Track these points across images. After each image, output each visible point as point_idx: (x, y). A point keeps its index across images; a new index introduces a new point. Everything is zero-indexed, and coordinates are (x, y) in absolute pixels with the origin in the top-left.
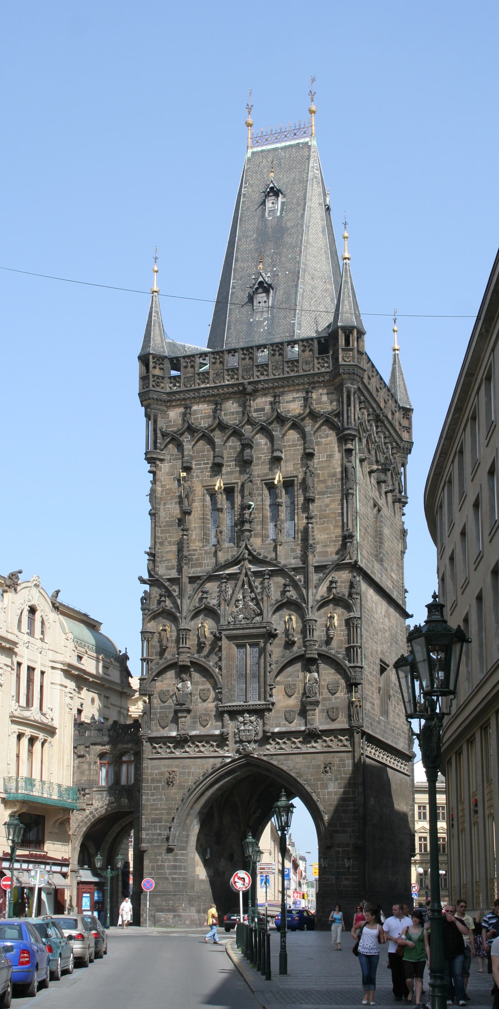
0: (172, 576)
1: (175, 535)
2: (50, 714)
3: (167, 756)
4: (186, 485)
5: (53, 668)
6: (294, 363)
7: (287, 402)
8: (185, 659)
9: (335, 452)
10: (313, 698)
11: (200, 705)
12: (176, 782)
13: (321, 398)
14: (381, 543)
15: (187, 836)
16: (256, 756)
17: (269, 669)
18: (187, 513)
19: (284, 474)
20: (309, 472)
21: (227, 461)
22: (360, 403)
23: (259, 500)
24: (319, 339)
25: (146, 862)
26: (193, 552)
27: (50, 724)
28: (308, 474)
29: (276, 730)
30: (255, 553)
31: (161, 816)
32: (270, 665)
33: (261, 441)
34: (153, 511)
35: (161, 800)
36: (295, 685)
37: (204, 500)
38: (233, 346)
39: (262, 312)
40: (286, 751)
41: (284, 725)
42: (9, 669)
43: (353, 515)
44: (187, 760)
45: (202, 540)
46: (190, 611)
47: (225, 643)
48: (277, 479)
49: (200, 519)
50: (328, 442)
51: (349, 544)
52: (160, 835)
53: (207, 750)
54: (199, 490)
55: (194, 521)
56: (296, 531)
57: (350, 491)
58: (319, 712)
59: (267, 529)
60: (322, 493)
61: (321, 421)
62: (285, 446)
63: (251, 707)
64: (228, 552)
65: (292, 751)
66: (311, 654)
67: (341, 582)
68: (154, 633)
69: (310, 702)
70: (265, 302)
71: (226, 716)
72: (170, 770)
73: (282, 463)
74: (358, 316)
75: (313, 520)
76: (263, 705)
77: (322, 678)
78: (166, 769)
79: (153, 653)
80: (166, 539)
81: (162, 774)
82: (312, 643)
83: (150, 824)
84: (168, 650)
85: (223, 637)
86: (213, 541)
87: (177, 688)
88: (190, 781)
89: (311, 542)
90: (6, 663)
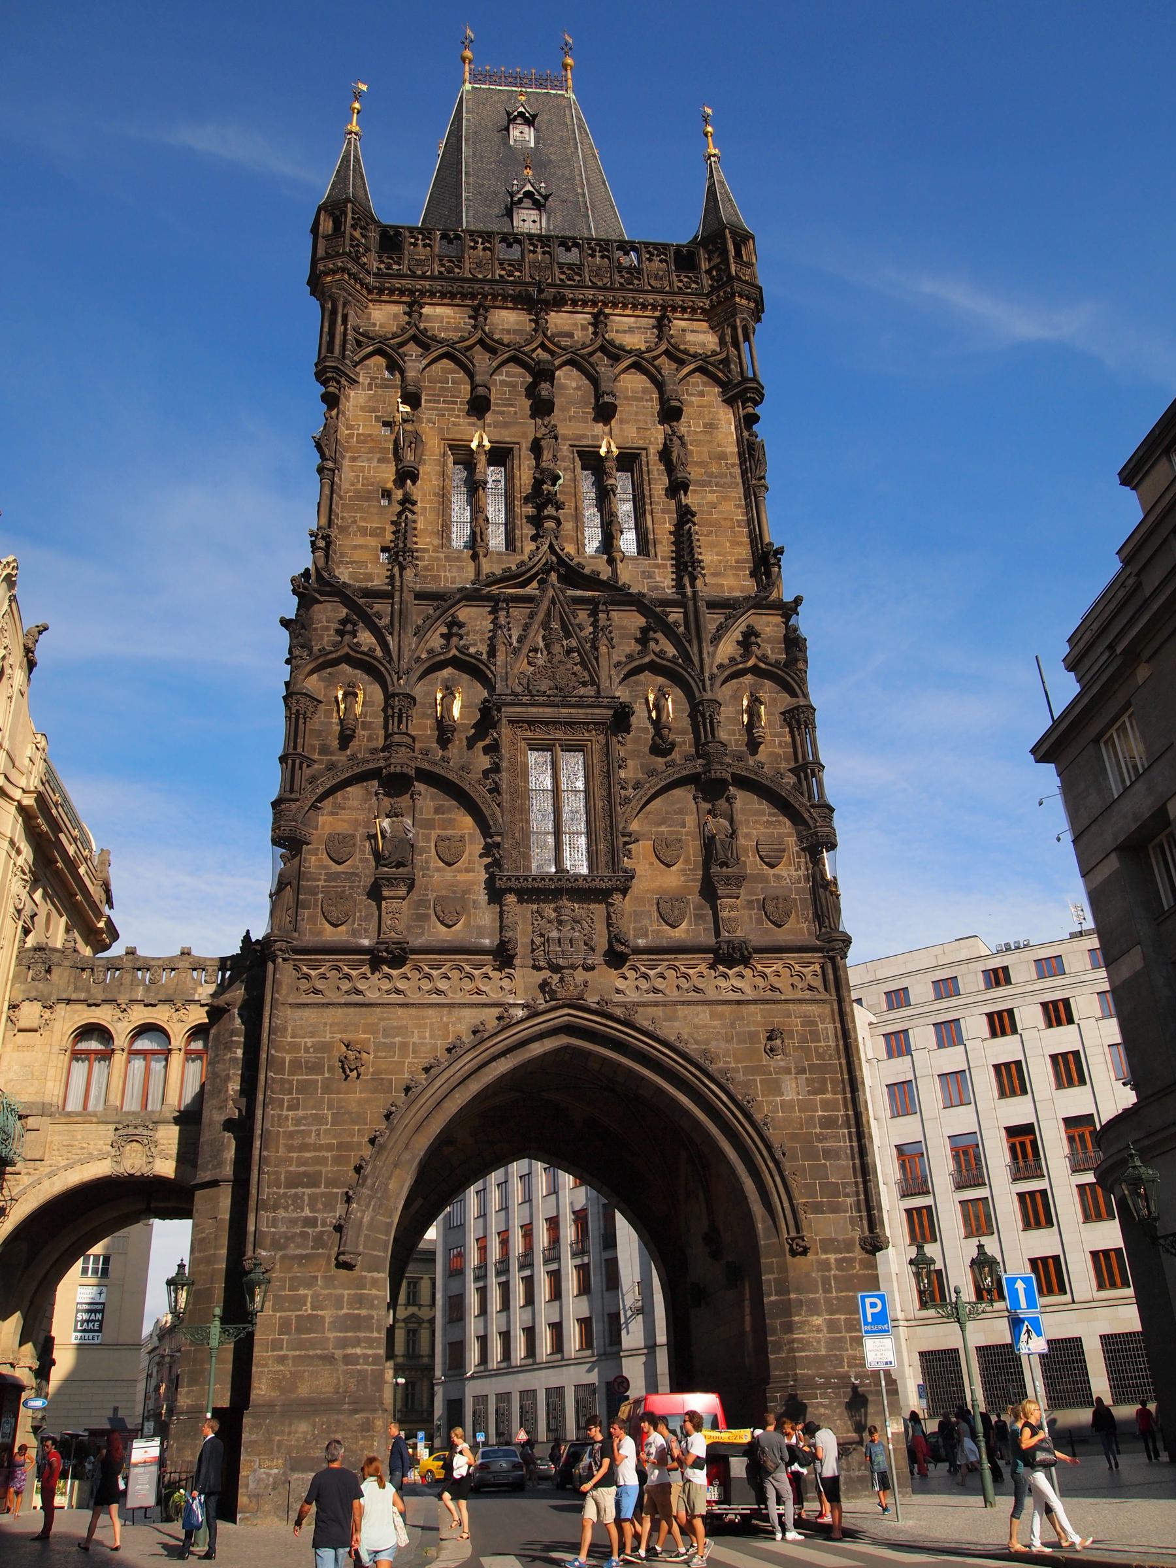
7: (617, 331)
8: (401, 761)
9: (719, 420)
11: (437, 875)
12: (368, 1072)
18: (407, 475)
19: (619, 441)
31: (317, 1168)
35: (320, 1120)
44: (400, 1011)
50: (705, 403)
52: (311, 1222)
53: (454, 987)
54: (434, 445)
61: (692, 367)
65: (681, 996)
68: (321, 702)
69: (728, 878)
70: (534, 221)
71: (511, 899)
72: (347, 1037)
73: (613, 422)
80: (355, 522)
81: (325, 1047)
83: (282, 1191)
85: (504, 721)
88: (408, 1068)
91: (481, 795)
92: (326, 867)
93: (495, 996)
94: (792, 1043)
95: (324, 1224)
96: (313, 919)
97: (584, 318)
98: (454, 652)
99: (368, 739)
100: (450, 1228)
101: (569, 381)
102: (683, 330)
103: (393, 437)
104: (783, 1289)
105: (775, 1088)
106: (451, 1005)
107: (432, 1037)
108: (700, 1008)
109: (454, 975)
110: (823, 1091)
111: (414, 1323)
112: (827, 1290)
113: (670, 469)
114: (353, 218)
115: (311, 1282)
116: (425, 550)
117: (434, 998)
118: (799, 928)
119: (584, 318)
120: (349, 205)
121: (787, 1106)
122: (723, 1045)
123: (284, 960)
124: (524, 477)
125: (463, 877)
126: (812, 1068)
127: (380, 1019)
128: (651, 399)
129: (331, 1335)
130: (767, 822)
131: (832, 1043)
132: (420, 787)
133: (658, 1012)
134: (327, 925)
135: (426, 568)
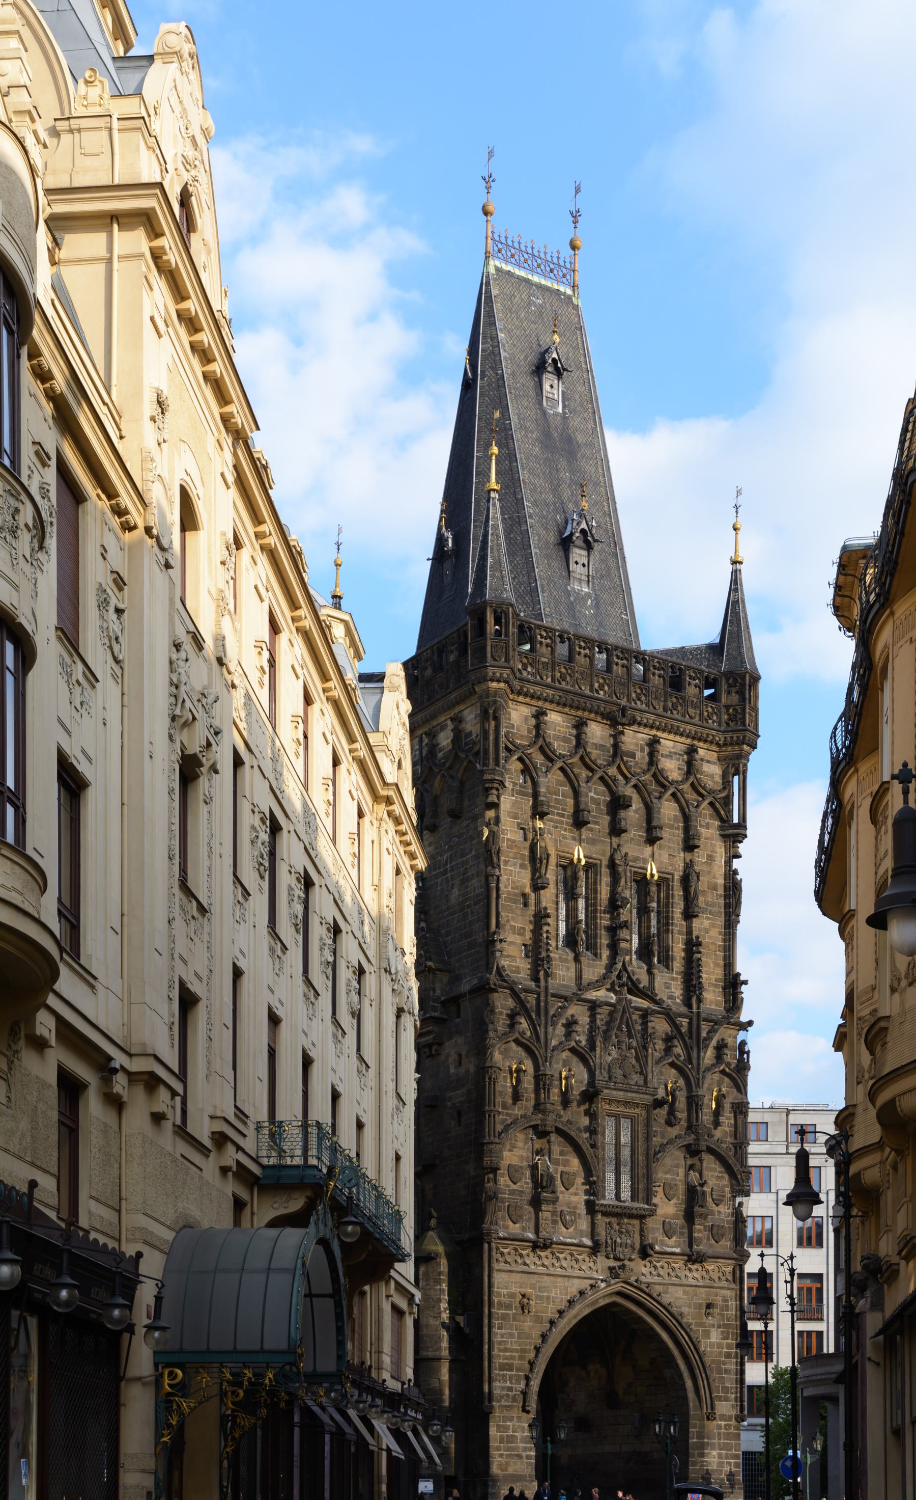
30: (634, 978)
35: (511, 1335)
41: (662, 1243)
44: (546, 1278)
80: (508, 921)
81: (512, 1295)
91: (586, 1147)
92: (508, 1186)
93: (588, 1273)
94: (717, 1311)
96: (503, 1217)
98: (573, 1044)
103: (527, 844)
104: (701, 1435)
105: (707, 1335)
106: (569, 1277)
108: (678, 1288)
110: (727, 1338)
112: (720, 1439)
117: (559, 1271)
118: (726, 1244)
121: (712, 1345)
124: (603, 893)
125: (574, 1199)
126: (725, 1326)
128: (678, 828)
130: (718, 1177)
131: (734, 1313)
132: (554, 1137)
134: (510, 1223)
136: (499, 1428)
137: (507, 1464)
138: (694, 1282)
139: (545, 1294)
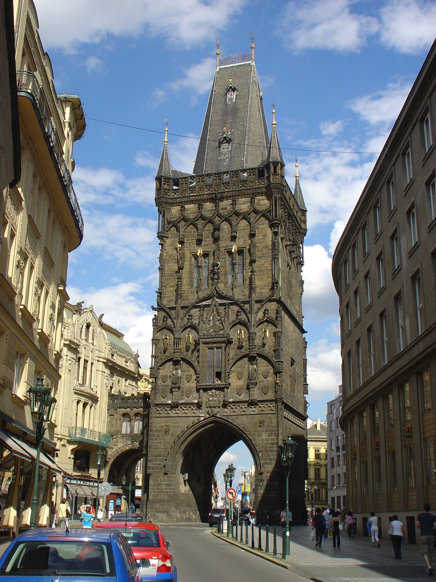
0: (171, 306)
1: (174, 282)
2: (95, 389)
3: (165, 416)
4: (180, 252)
5: (98, 361)
6: (245, 181)
7: (240, 204)
8: (177, 356)
10: (254, 381)
12: (170, 432)
13: (260, 202)
14: (291, 288)
15: (176, 466)
16: (218, 416)
17: (227, 363)
18: (181, 268)
19: (238, 246)
20: (253, 245)
21: (205, 238)
22: (281, 205)
23: (223, 261)
24: (259, 169)
25: (151, 482)
26: (183, 292)
27: (95, 395)
28: (252, 246)
29: (231, 400)
30: (220, 293)
32: (228, 360)
33: (225, 226)
34: (161, 267)
35: (161, 443)
36: (243, 372)
37: (191, 261)
38: (209, 172)
39: (226, 154)
40: (237, 413)
42: (74, 361)
43: (277, 270)
45: (189, 285)
46: (181, 327)
47: (202, 346)
48: (234, 249)
49: (188, 272)
51: (276, 287)
52: (160, 464)
53: (189, 412)
54: (188, 255)
55: (185, 273)
56: (244, 280)
57: (276, 256)
58: (257, 389)
59: (227, 279)
60: (260, 257)
62: (239, 230)
63: (216, 386)
64: (204, 292)
66: (253, 353)
67: (271, 310)
68: (159, 340)
69: (252, 383)
71: (201, 391)
72: (166, 424)
74: (281, 157)
75: (255, 273)
76: (223, 385)
77: (259, 369)
78: (165, 424)
79: (158, 352)
81: (162, 427)
82: (253, 347)
84: (168, 350)
85: (201, 343)
86: (195, 285)
87: (173, 374)
88: (179, 432)
89: (253, 286)
90: (73, 357)
92: (162, 383)
93: (198, 414)
94: (266, 424)
95: (162, 465)
96: (159, 396)
97: (230, 202)
98: (190, 324)
99: (170, 350)
100: (331, 431)
101: (225, 226)
102: (260, 200)
105: (260, 435)
107: (184, 424)
108: (244, 416)
109: (189, 409)
111: (318, 466)
113: (250, 255)
114: (164, 181)
115: (159, 477)
116: (185, 291)
117: (185, 415)
119: (230, 202)
120: (163, 178)
121: (262, 440)
122: (249, 425)
123: (153, 407)
125: (192, 385)
127: (173, 420)
129: (163, 487)
133: (234, 417)
135: (186, 296)
136: (154, 481)
137: (157, 495)
138: (253, 413)
139: (177, 425)
